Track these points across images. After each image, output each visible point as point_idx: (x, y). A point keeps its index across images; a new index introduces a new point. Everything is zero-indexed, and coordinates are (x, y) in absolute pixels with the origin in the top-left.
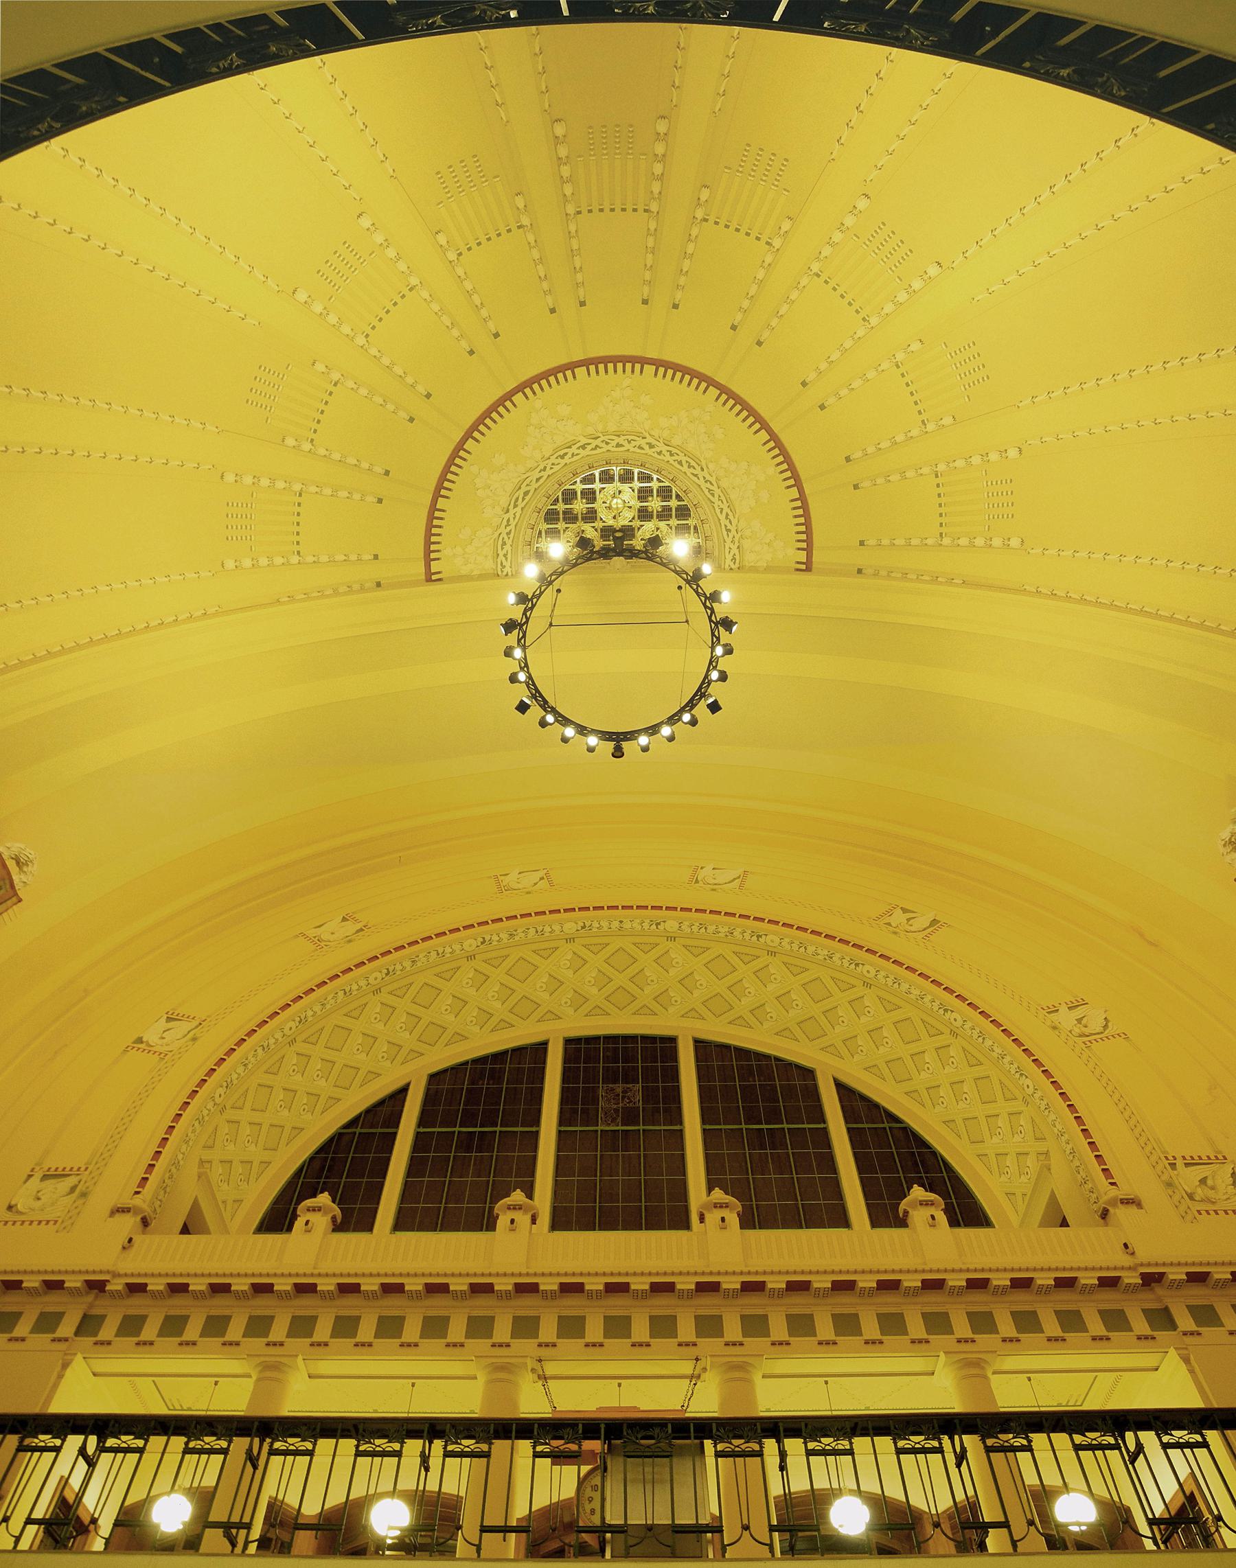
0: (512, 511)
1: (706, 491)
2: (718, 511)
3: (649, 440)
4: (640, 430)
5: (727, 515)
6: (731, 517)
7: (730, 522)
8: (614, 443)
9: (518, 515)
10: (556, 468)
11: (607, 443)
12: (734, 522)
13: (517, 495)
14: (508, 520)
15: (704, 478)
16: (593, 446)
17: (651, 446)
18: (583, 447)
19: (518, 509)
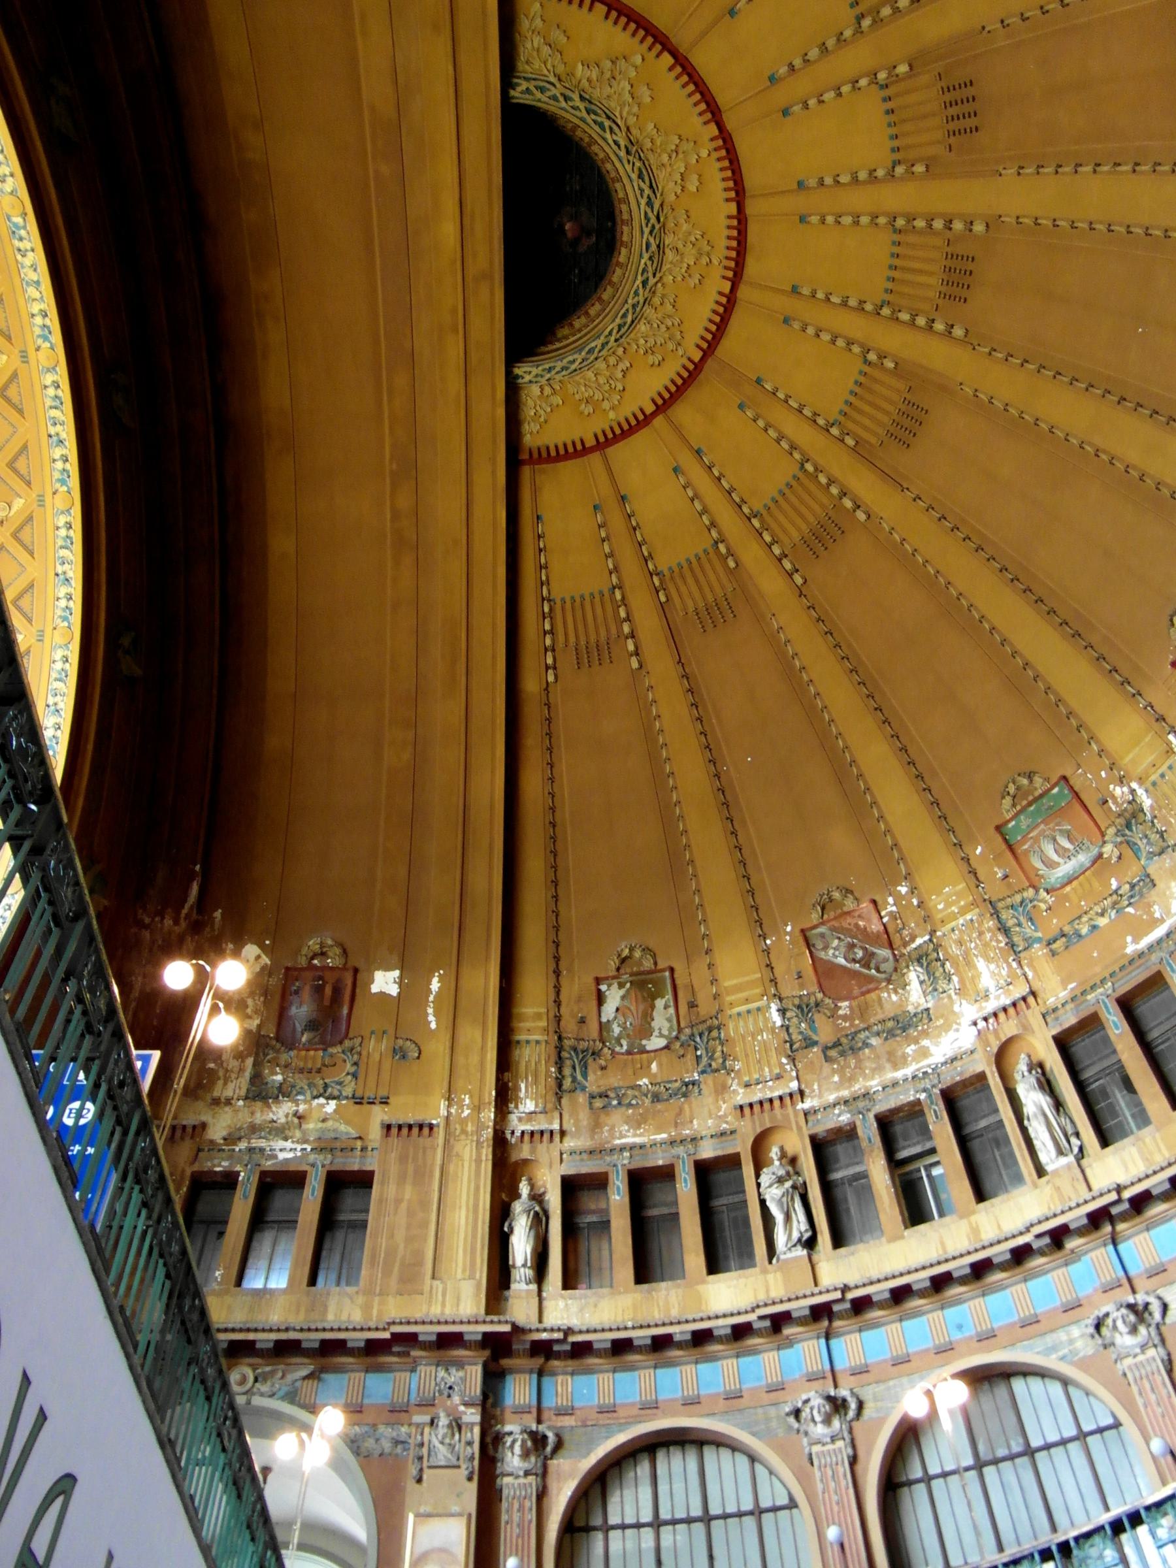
0: (582, 106)
1: (593, 345)
2: (571, 358)
3: (652, 281)
4: (664, 268)
5: (567, 368)
6: (564, 373)
7: (558, 373)
8: (652, 240)
9: (577, 113)
10: (629, 168)
11: (651, 233)
12: (558, 377)
13: (599, 111)
14: (571, 99)
15: (607, 343)
16: (650, 214)
17: (645, 283)
18: (650, 204)
19: (584, 114)
